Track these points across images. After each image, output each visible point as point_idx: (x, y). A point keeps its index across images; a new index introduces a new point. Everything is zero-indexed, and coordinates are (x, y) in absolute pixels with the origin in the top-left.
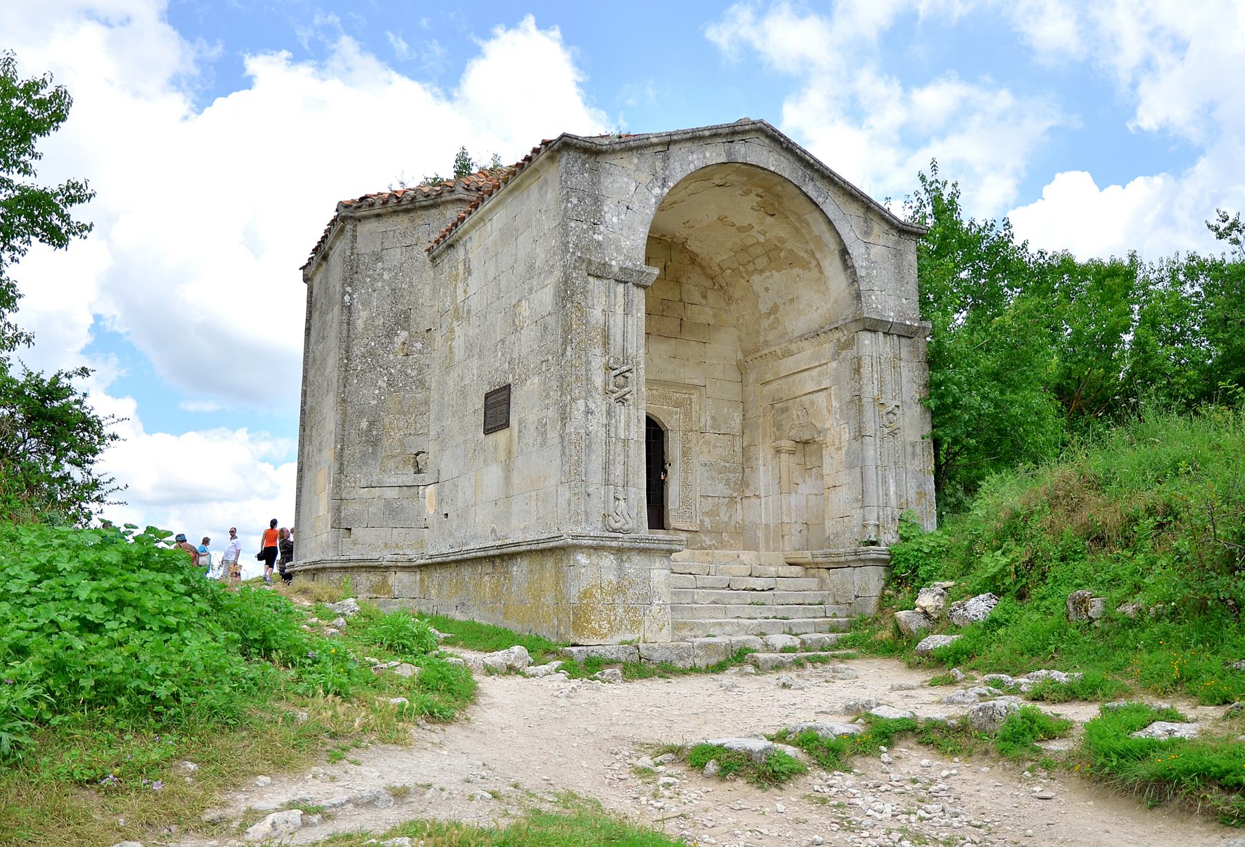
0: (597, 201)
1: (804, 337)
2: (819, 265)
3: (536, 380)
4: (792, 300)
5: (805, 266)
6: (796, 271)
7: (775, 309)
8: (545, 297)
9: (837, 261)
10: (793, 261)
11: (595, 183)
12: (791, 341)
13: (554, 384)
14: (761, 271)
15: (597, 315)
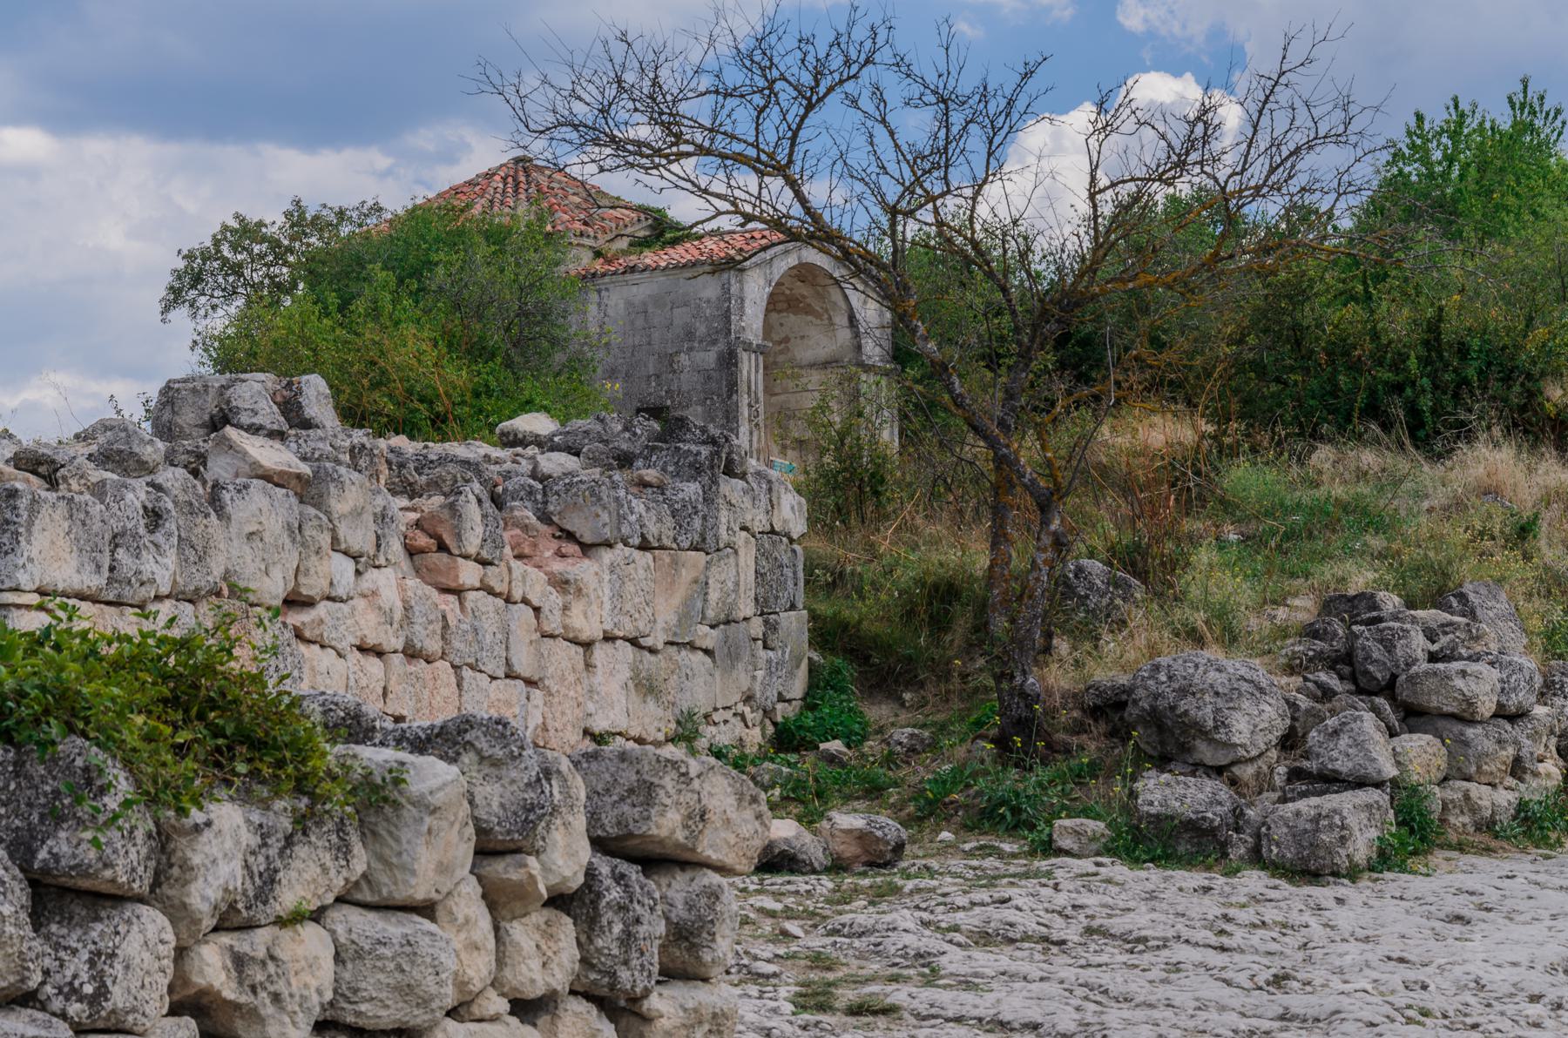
0: (743, 300)
1: (812, 366)
2: (830, 318)
3: (699, 409)
4: (802, 337)
5: (818, 316)
6: (810, 318)
7: (786, 340)
8: (709, 358)
9: (845, 321)
10: (809, 311)
11: (742, 289)
12: (801, 367)
13: (720, 414)
14: (780, 311)
15: (745, 373)
